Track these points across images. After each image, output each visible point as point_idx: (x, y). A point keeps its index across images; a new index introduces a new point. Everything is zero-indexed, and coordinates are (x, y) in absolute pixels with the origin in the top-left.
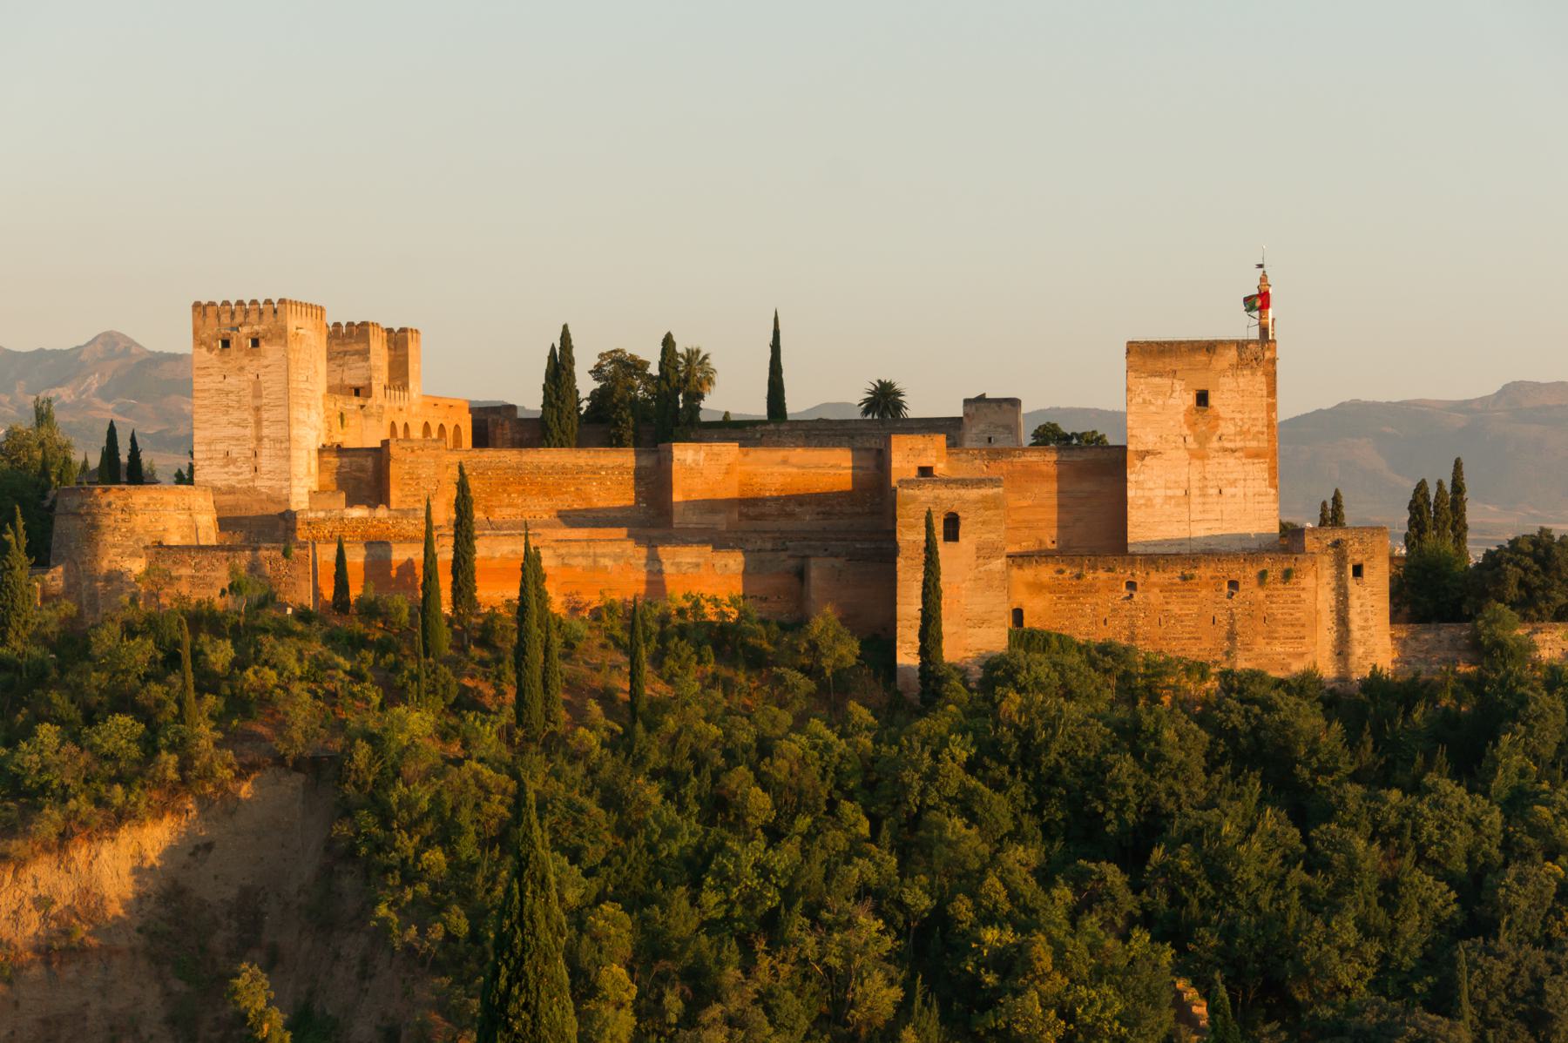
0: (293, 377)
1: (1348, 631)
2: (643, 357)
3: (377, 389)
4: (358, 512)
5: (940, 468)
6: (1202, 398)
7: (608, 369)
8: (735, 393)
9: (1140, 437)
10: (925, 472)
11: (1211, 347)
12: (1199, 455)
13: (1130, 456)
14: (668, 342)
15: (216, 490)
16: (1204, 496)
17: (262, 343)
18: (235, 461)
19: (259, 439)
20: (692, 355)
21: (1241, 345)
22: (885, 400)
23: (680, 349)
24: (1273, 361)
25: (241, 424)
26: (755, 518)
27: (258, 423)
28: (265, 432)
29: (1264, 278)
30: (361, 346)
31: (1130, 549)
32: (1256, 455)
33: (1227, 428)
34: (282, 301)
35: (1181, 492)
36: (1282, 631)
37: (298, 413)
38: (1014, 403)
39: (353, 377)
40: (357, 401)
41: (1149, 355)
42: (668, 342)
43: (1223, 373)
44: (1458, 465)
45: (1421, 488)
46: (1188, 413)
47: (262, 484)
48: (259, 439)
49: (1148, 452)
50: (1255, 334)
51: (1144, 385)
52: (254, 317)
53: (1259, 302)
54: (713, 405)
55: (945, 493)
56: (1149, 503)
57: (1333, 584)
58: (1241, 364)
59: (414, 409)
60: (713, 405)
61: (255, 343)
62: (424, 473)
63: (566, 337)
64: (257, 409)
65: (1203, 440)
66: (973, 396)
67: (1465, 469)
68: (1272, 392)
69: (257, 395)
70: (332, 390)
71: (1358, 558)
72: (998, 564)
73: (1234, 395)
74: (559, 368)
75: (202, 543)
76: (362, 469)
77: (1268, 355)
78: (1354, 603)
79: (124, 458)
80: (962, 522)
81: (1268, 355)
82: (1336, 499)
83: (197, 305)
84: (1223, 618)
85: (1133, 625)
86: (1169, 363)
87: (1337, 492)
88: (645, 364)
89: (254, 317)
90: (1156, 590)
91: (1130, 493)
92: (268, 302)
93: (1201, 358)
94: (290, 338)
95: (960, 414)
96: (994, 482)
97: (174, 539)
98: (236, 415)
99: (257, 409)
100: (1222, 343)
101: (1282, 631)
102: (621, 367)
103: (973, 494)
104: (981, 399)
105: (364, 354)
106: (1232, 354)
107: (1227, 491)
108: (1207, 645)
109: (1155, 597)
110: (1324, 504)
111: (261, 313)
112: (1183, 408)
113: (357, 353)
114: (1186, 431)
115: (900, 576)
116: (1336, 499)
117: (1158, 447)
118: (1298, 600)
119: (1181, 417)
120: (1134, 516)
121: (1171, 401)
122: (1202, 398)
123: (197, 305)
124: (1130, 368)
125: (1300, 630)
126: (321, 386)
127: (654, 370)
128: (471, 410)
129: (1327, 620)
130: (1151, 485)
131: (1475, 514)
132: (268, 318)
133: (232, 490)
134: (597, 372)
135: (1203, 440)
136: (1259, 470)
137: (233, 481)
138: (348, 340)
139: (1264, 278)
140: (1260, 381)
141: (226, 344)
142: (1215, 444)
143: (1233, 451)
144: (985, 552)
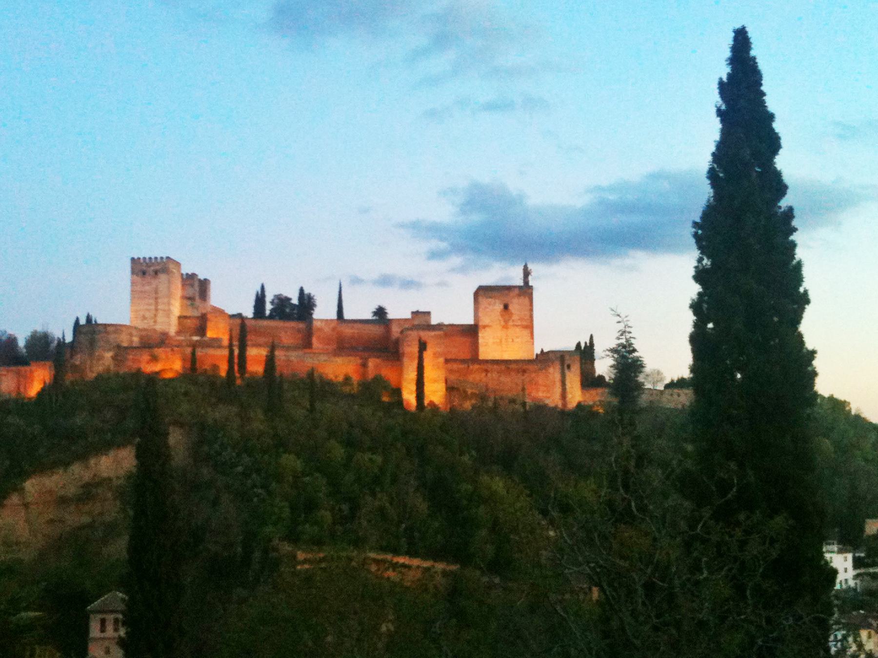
2: (289, 296)
3: (197, 298)
6: (506, 307)
7: (276, 301)
8: (324, 312)
11: (509, 288)
12: (505, 327)
14: (302, 290)
15: (141, 330)
19: (157, 310)
21: (520, 287)
22: (380, 312)
23: (306, 291)
24: (532, 294)
27: (157, 303)
32: (526, 327)
33: (515, 317)
36: (542, 388)
37: (173, 302)
38: (429, 313)
42: (302, 290)
44: (591, 337)
48: (157, 310)
50: (522, 284)
58: (519, 295)
66: (415, 310)
67: (594, 338)
69: (156, 292)
73: (516, 306)
74: (260, 300)
75: (134, 345)
83: (133, 259)
86: (495, 294)
88: (289, 299)
93: (506, 292)
95: (409, 316)
97: (125, 344)
99: (156, 298)
102: (282, 302)
103: (433, 333)
105: (192, 286)
106: (517, 291)
107: (516, 340)
109: (495, 375)
120: (481, 350)
122: (506, 307)
123: (133, 259)
127: (295, 301)
133: (145, 330)
134: (272, 303)
135: (506, 322)
137: (145, 327)
138: (190, 279)
140: (526, 301)
141: (144, 273)
142: (511, 323)
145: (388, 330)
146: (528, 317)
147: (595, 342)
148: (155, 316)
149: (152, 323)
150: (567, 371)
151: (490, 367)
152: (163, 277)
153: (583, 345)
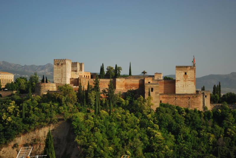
0: (67, 69)
1: (204, 104)
3: (78, 71)
4: (75, 87)
5: (151, 82)
6: (186, 73)
9: (177, 78)
10: (149, 82)
11: (187, 67)
12: (185, 81)
13: (176, 81)
14: (116, 65)
15: (56, 84)
16: (186, 86)
17: (63, 65)
18: (59, 80)
19: (62, 77)
20: (119, 67)
21: (191, 67)
23: (118, 66)
24: (195, 69)
25: (60, 75)
26: (127, 88)
28: (63, 76)
29: (194, 58)
30: (76, 65)
31: (176, 93)
32: (193, 81)
33: (189, 77)
34: (65, 59)
35: (182, 86)
36: (196, 104)
37: (67, 74)
39: (75, 69)
40: (75, 72)
41: (179, 68)
42: (116, 65)
43: (188, 70)
44: (220, 83)
45: (215, 86)
46: (184, 75)
47: (62, 83)
49: (178, 80)
51: (178, 72)
52: (62, 61)
53: (194, 61)
54: (122, 73)
55: (151, 85)
56: (178, 87)
57: (203, 98)
59: (83, 73)
60: (122, 73)
61: (62, 65)
62: (83, 82)
63: (103, 64)
64: (62, 73)
65: (186, 79)
68: (195, 73)
69: (62, 71)
70: (72, 71)
71: (206, 95)
72: (158, 95)
73: (190, 73)
75: (54, 90)
76: (76, 81)
77: (194, 68)
78: (205, 100)
79: (45, 80)
80: (154, 89)
81: (194, 68)
82: (204, 87)
83: (54, 60)
84: (188, 102)
85: (176, 103)
87: (204, 86)
89: (62, 61)
90: (179, 98)
91: (176, 86)
92: (64, 59)
93: (185, 68)
94: (66, 64)
96: (158, 84)
98: (59, 74)
99: (62, 73)
100: (188, 66)
101: (196, 104)
102: (110, 69)
103: (155, 85)
104: (157, 73)
105: (76, 66)
106: (190, 68)
107: (189, 86)
108: (186, 106)
110: (202, 88)
111: (63, 61)
112: (183, 75)
113: (75, 66)
114: (183, 78)
115: (145, 96)
116: (204, 87)
117: (180, 80)
118: (198, 100)
119: (183, 76)
120: (176, 89)
121: (181, 74)
122: (186, 73)
123: (54, 60)
124: (176, 69)
125: (198, 104)
126: (71, 70)
127: (114, 69)
128: (91, 74)
129: (202, 103)
130: (179, 85)
131: (222, 89)
132: (64, 61)
133: (58, 84)
134: (107, 69)
135: (186, 79)
136: (193, 83)
137: (59, 82)
139: (194, 58)
140: (193, 71)
141: (58, 65)
143: (190, 80)
144: (157, 93)
145: (143, 81)
146: (193, 77)
147: (221, 85)
148: (62, 79)
149: (60, 81)
150: (205, 98)
151: (177, 96)
152: (64, 66)
153: (216, 86)
